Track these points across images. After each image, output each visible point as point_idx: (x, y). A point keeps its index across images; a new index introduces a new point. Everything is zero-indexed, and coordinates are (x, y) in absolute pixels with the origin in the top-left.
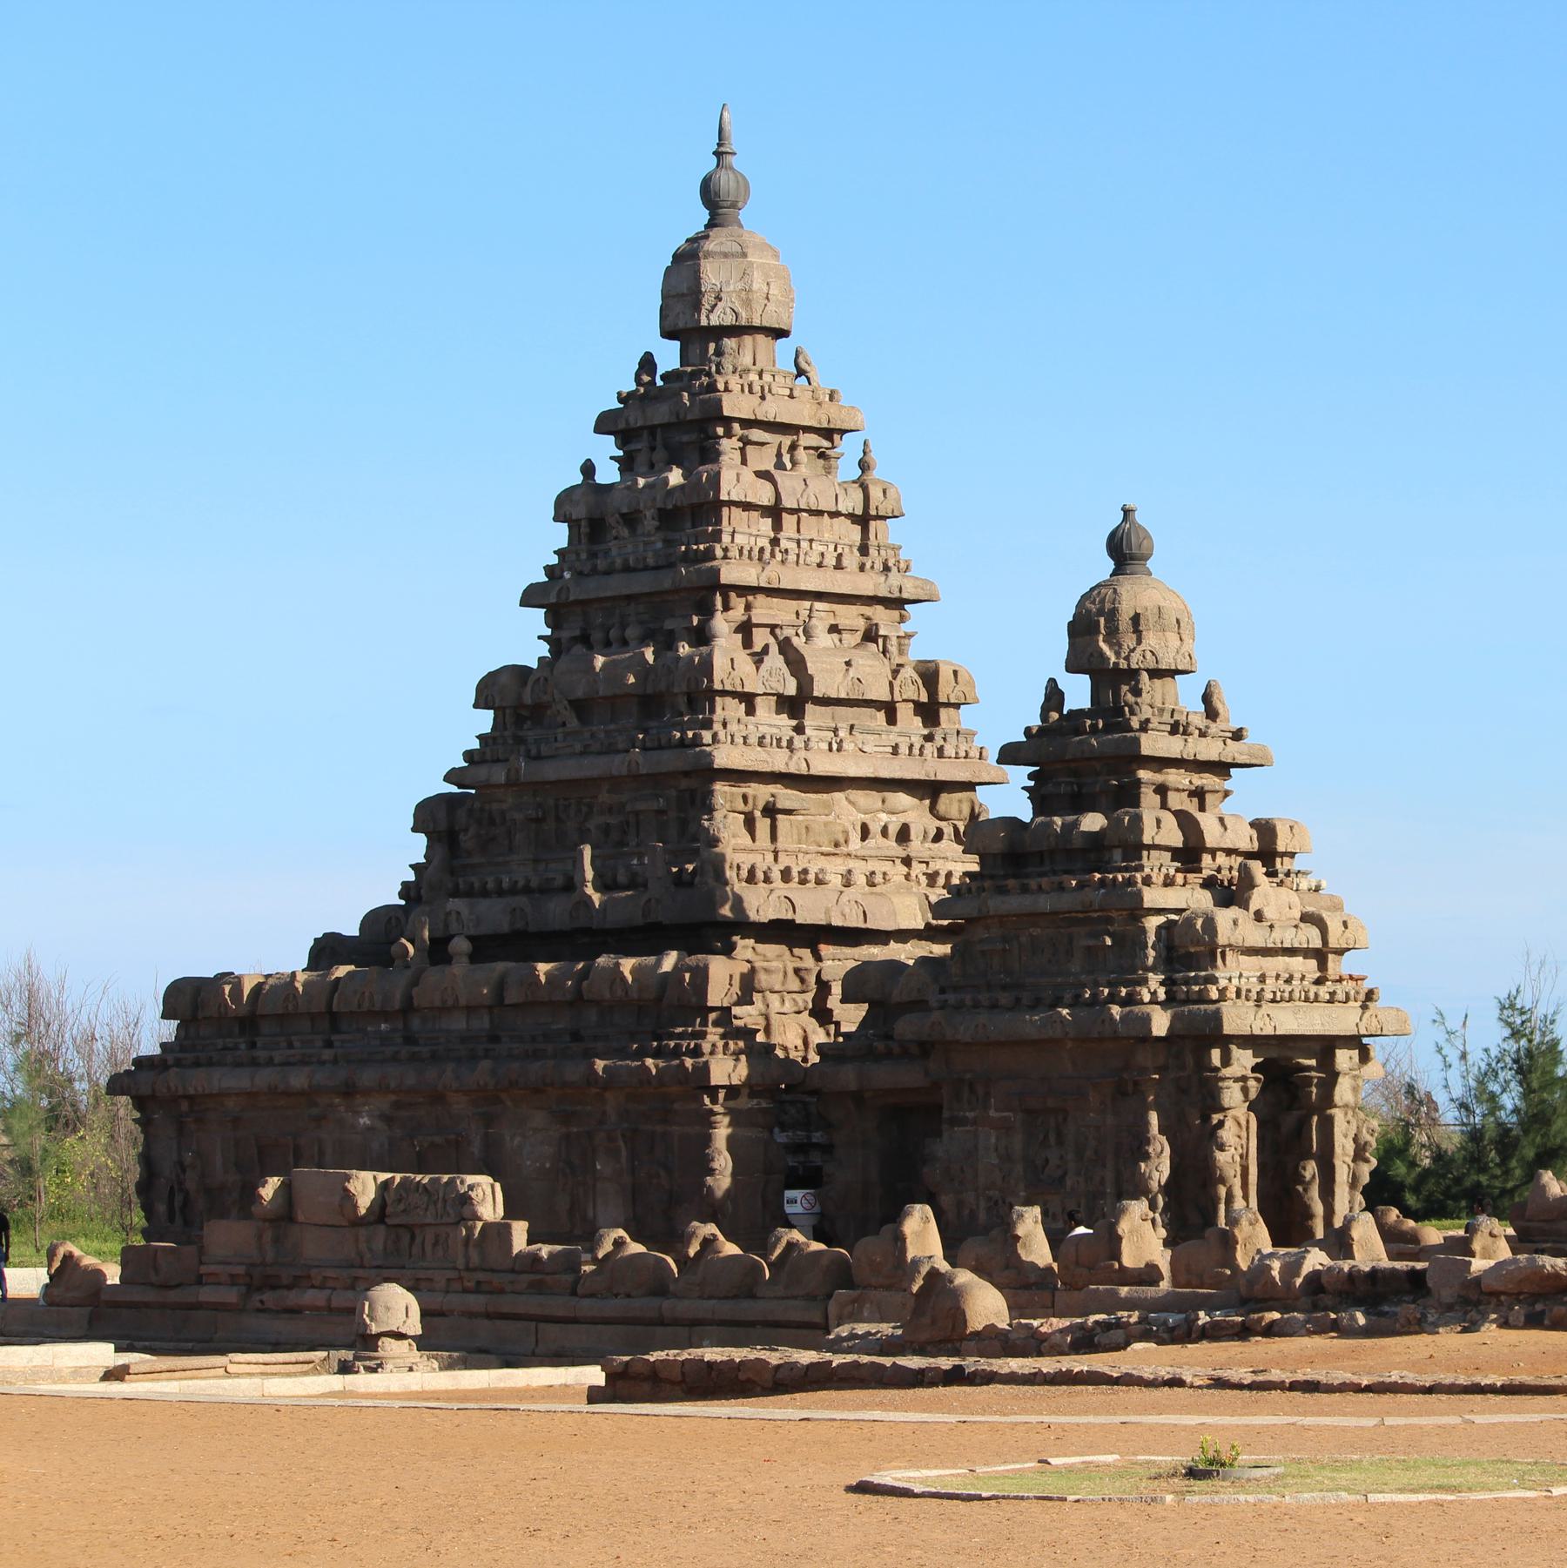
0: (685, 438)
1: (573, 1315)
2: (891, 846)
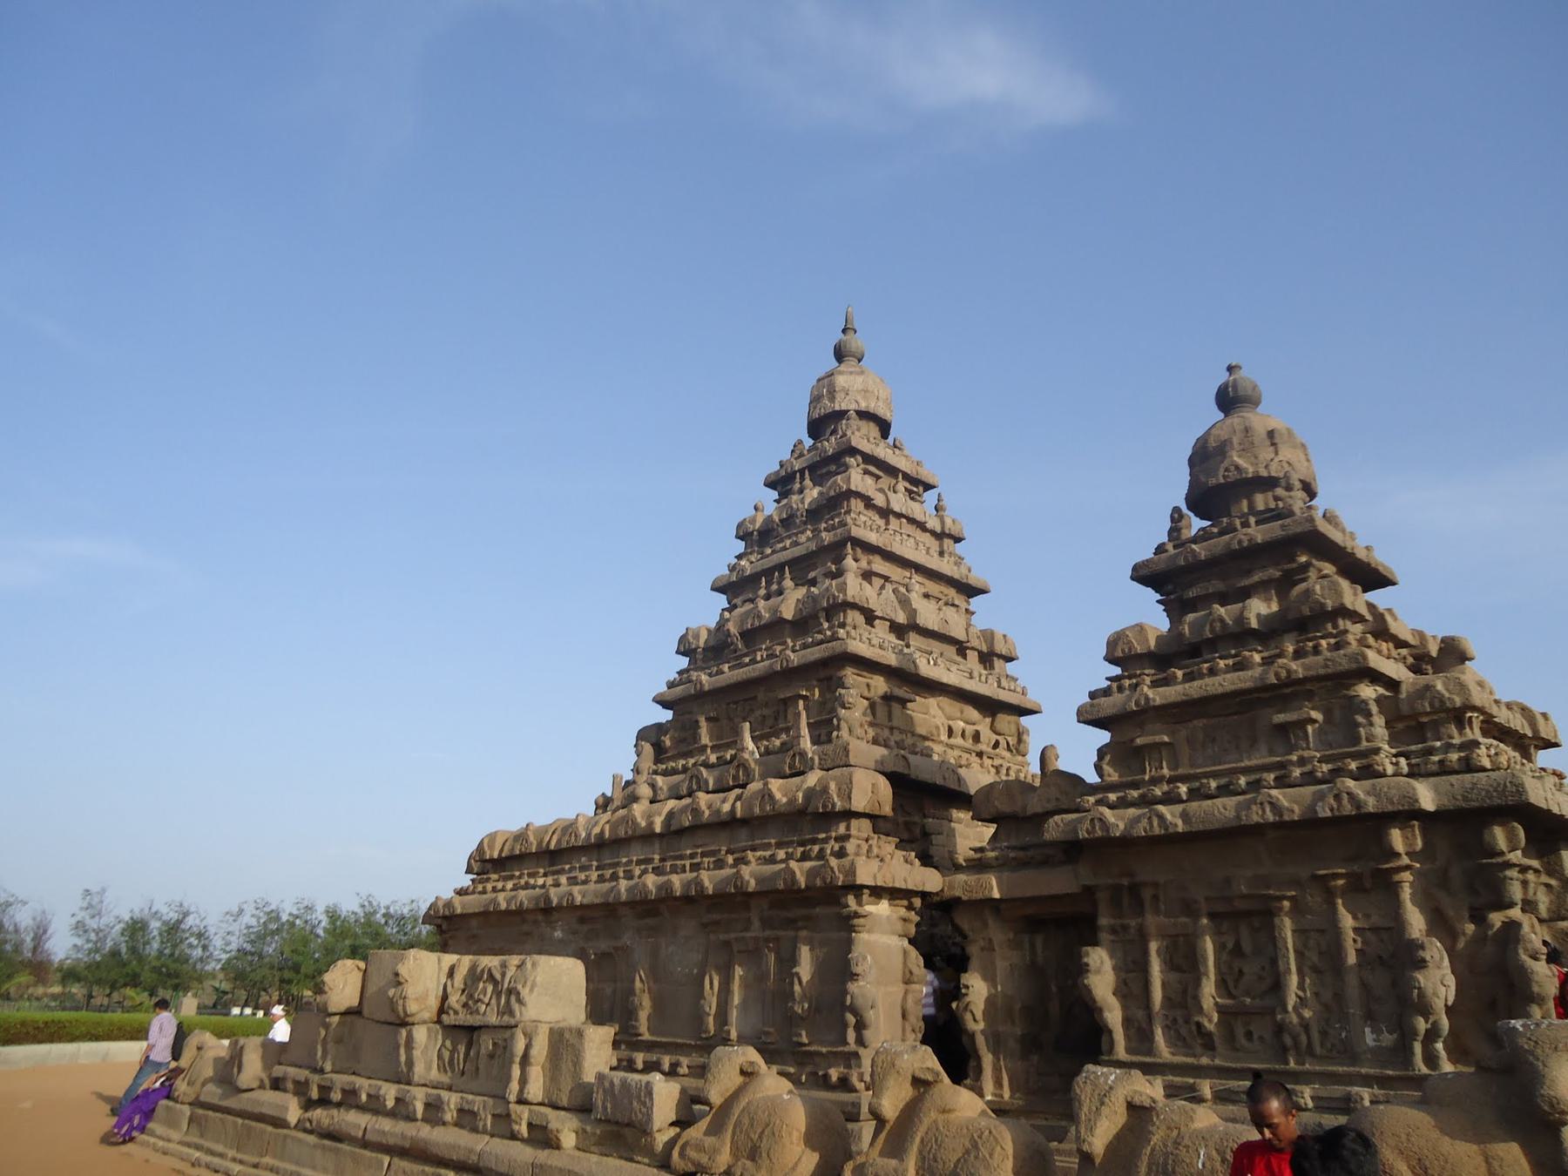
2: (969, 744)
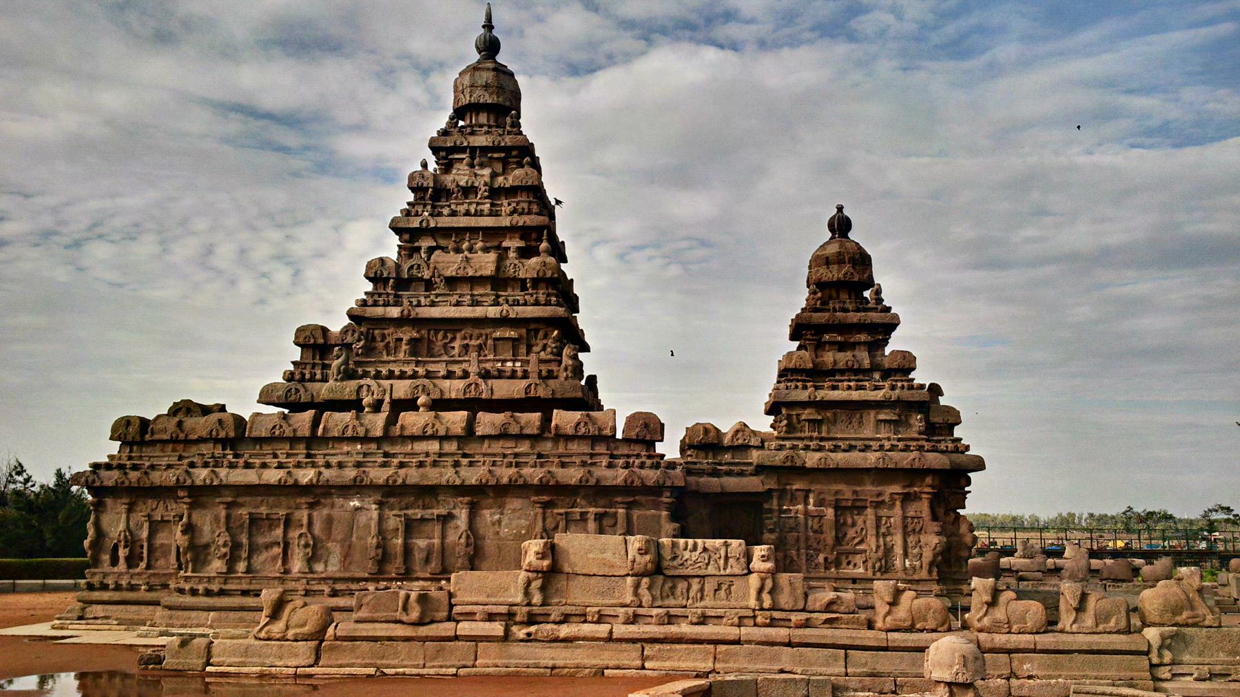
0: (495, 155)
1: (885, 645)
